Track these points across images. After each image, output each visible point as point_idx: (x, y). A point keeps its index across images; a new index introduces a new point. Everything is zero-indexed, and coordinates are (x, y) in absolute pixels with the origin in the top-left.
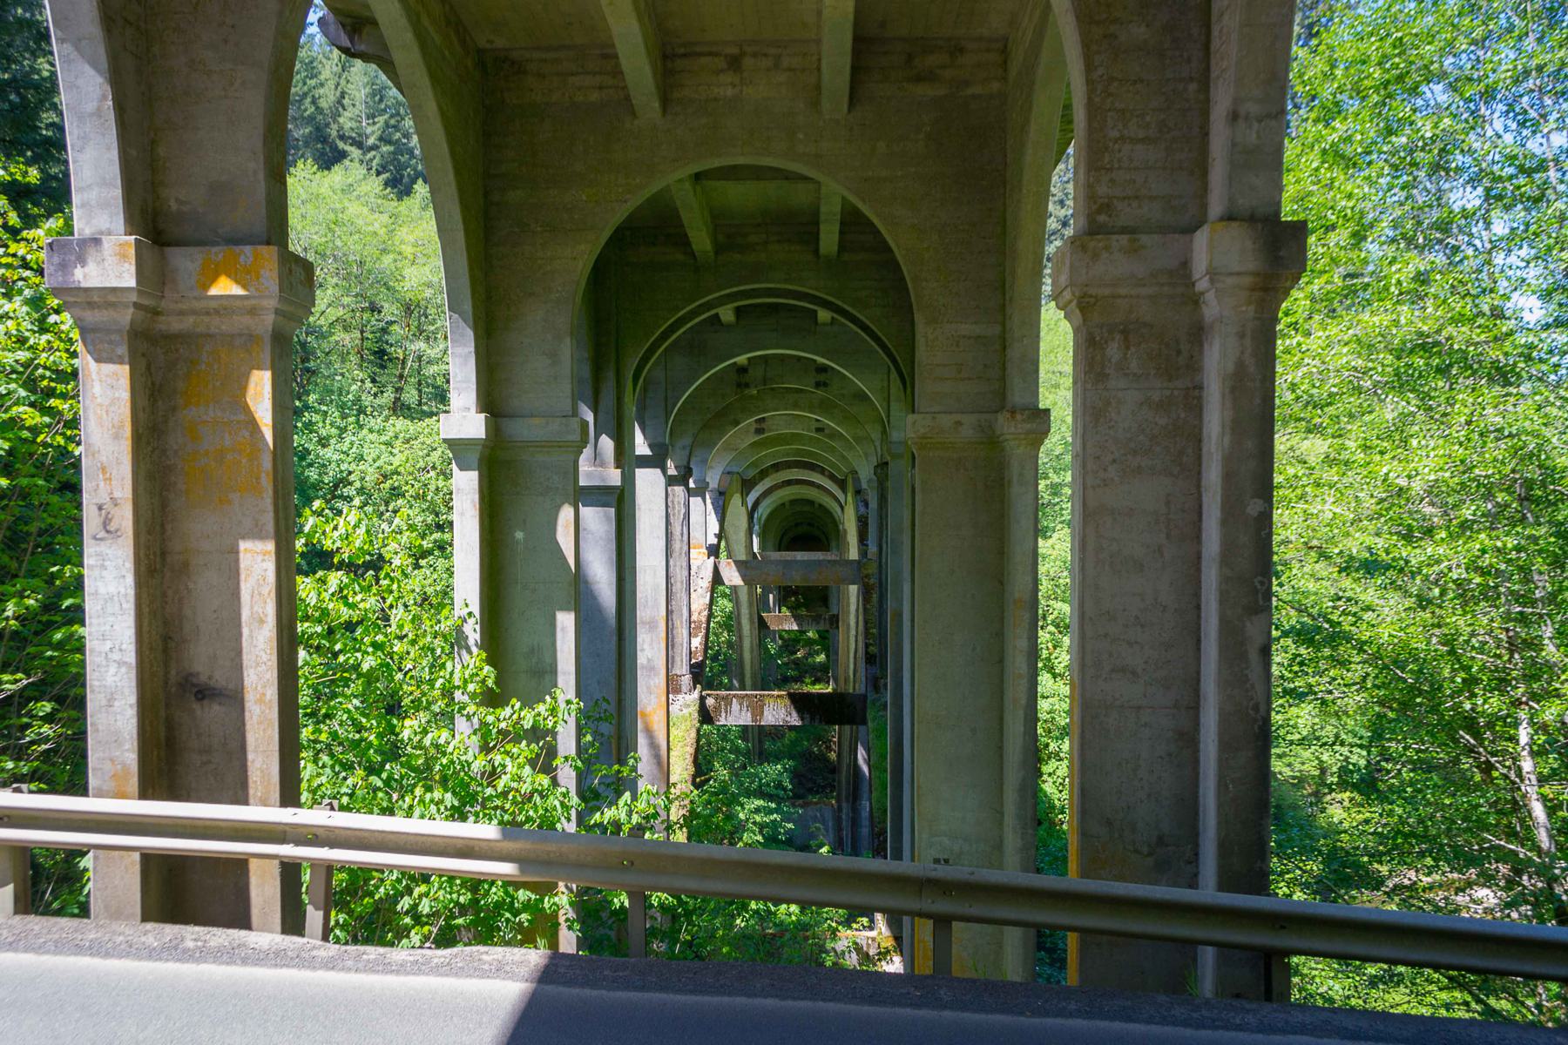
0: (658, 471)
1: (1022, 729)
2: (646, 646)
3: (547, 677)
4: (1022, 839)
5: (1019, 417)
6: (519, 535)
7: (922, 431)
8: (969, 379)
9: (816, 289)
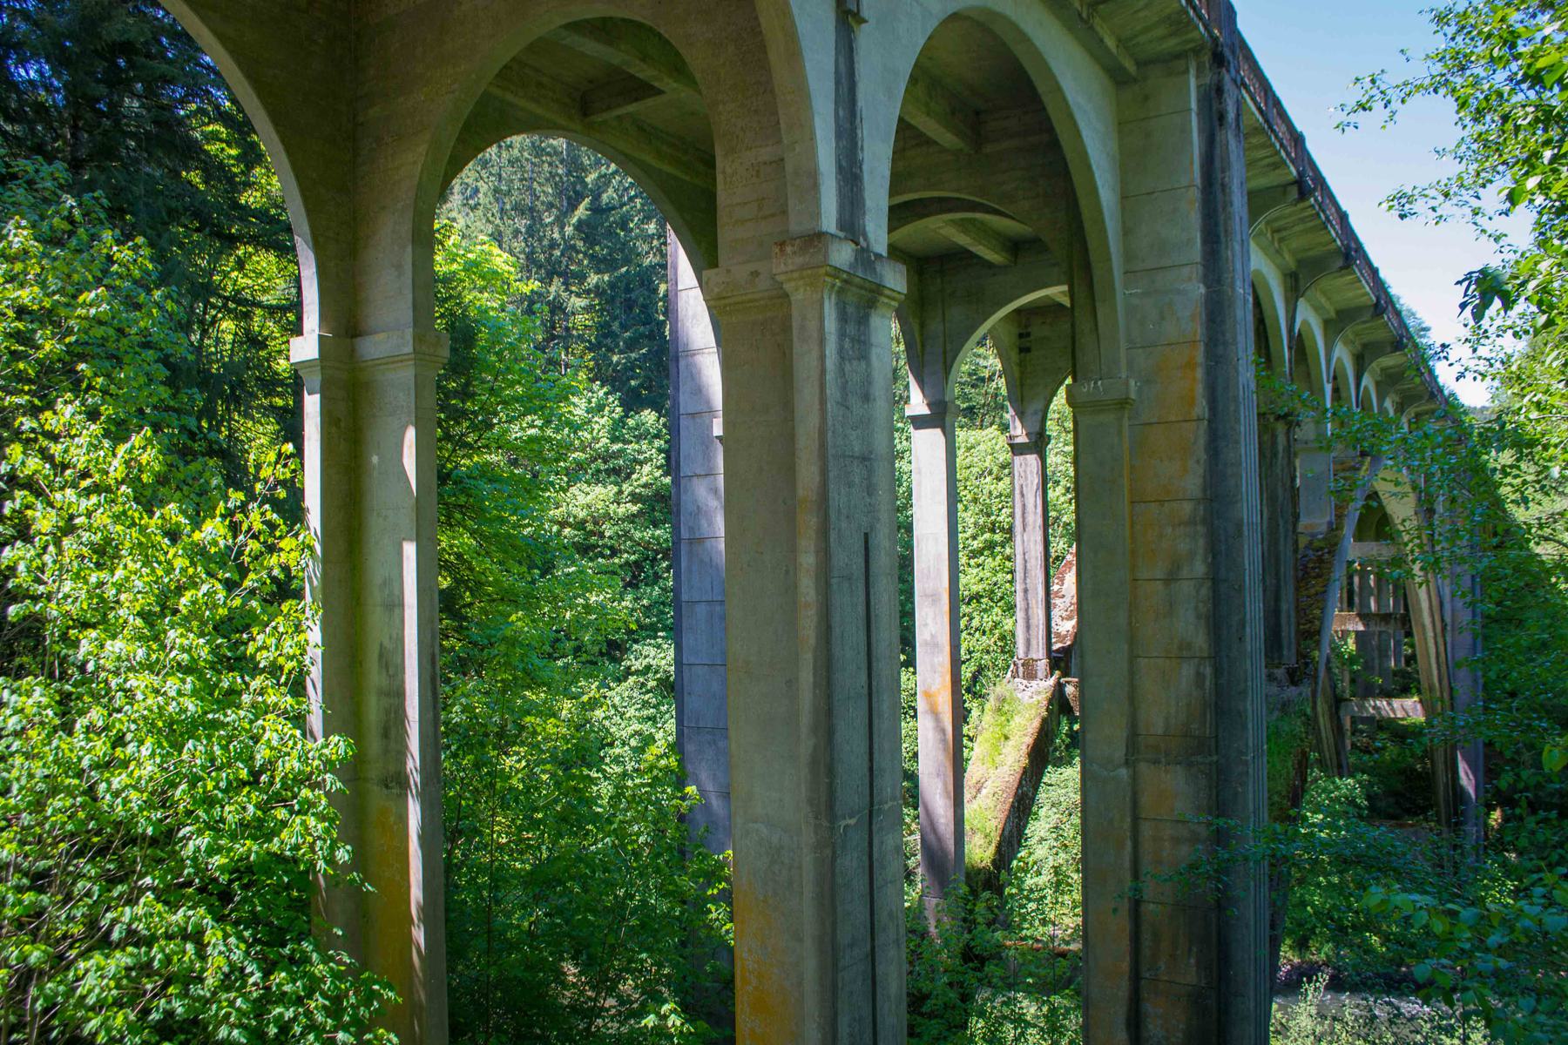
0: (938, 431)
1: (811, 680)
2: (929, 621)
3: (397, 611)
4: (816, 833)
5: (789, 249)
6: (375, 459)
7: (716, 290)
8: (773, 215)
9: (958, 191)
